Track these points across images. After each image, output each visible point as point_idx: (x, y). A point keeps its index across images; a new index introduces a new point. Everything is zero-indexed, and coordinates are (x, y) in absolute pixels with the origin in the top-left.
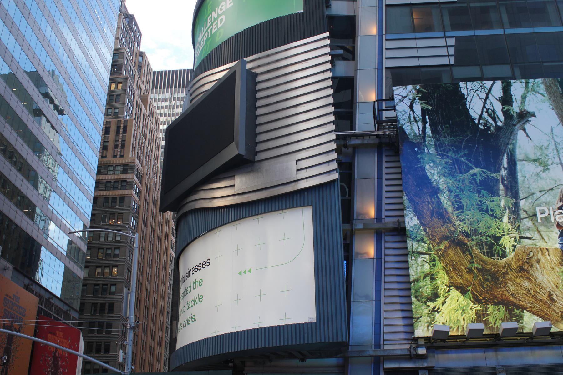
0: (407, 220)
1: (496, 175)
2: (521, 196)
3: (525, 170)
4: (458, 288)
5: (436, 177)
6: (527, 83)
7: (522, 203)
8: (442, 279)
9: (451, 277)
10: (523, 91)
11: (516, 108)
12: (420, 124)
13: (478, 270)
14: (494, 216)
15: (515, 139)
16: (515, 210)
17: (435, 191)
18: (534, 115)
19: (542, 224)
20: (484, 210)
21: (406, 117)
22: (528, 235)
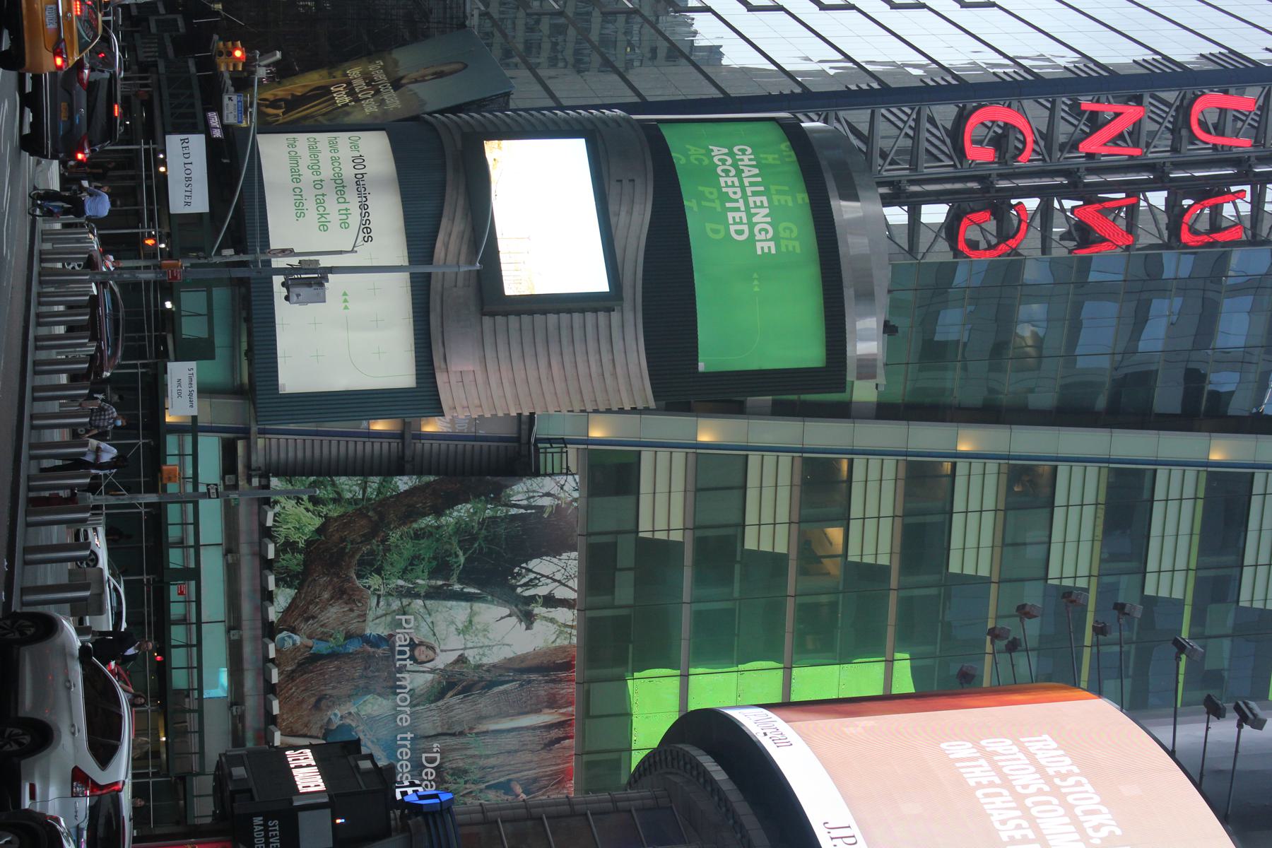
0: (405, 478)
1: (455, 577)
2: (428, 602)
3: (460, 611)
4: (323, 525)
5: (455, 514)
6: (572, 627)
7: (420, 602)
8: (334, 511)
9: (336, 519)
10: (561, 621)
11: (539, 610)
12: (525, 502)
13: (344, 548)
14: (405, 571)
15: (499, 604)
16: (412, 594)
17: (439, 513)
18: (527, 628)
19: (394, 619)
20: (414, 560)
21: (535, 487)
22: (382, 603)
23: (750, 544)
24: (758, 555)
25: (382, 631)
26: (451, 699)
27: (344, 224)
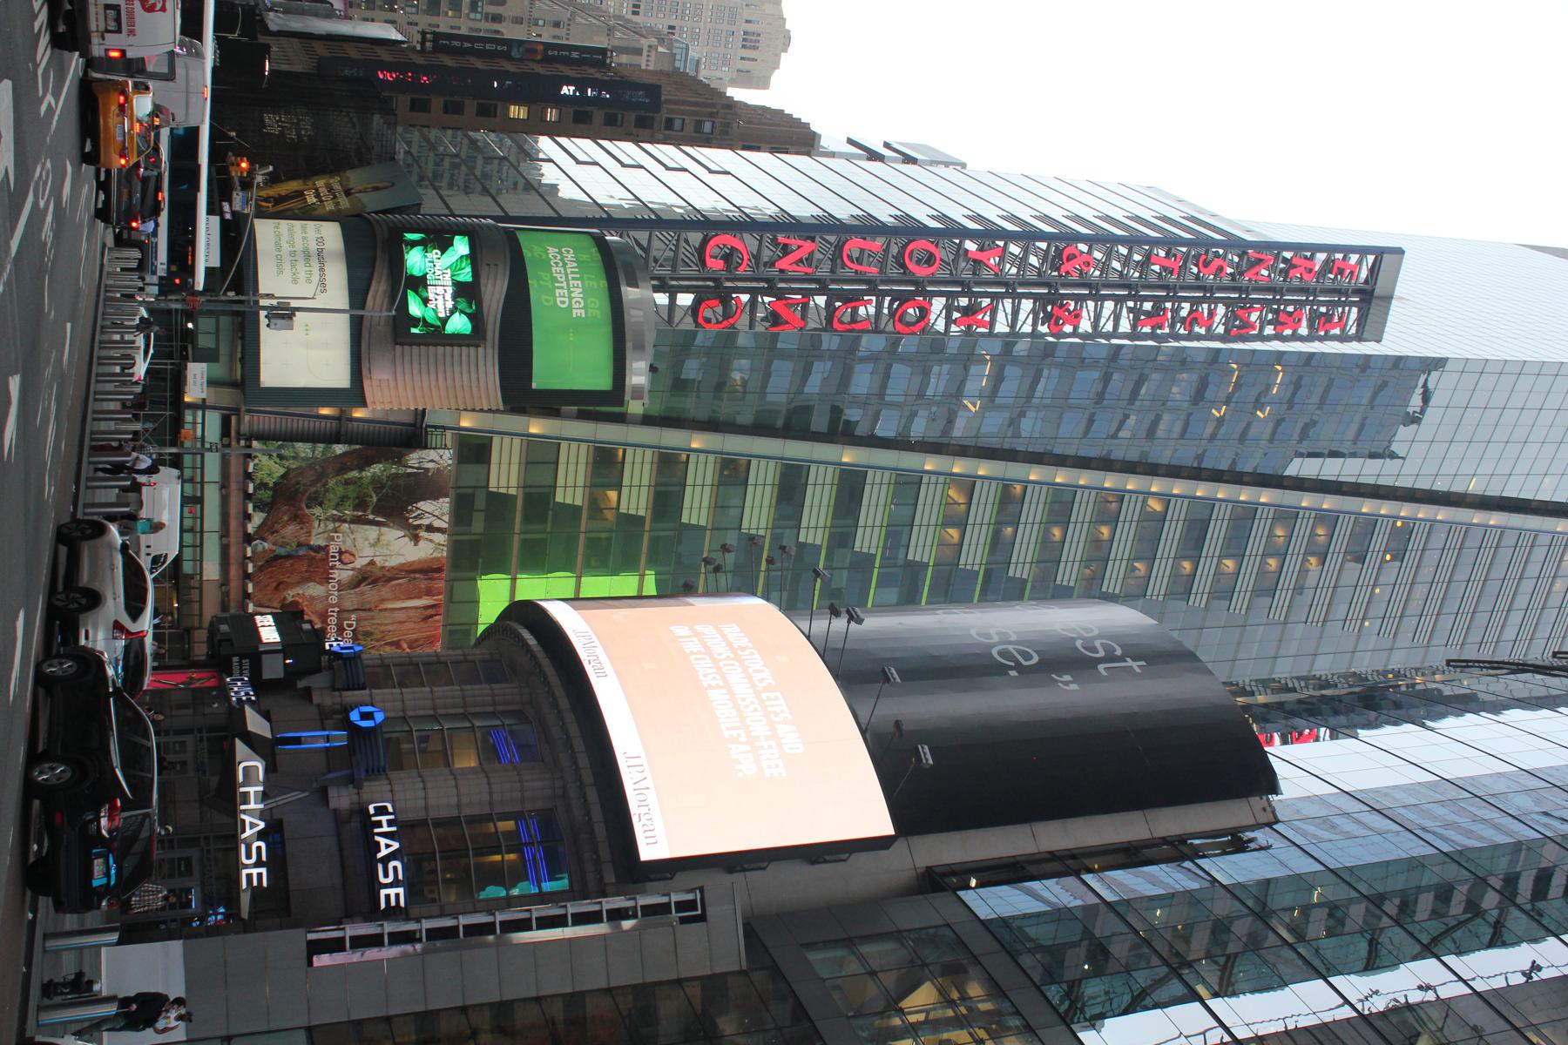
3: (372, 532)
8: (293, 465)
11: (423, 534)
16: (342, 520)
17: (361, 469)
20: (344, 499)
23: (559, 499)
24: (563, 505)
25: (322, 543)
26: (364, 588)
27: (309, 281)
